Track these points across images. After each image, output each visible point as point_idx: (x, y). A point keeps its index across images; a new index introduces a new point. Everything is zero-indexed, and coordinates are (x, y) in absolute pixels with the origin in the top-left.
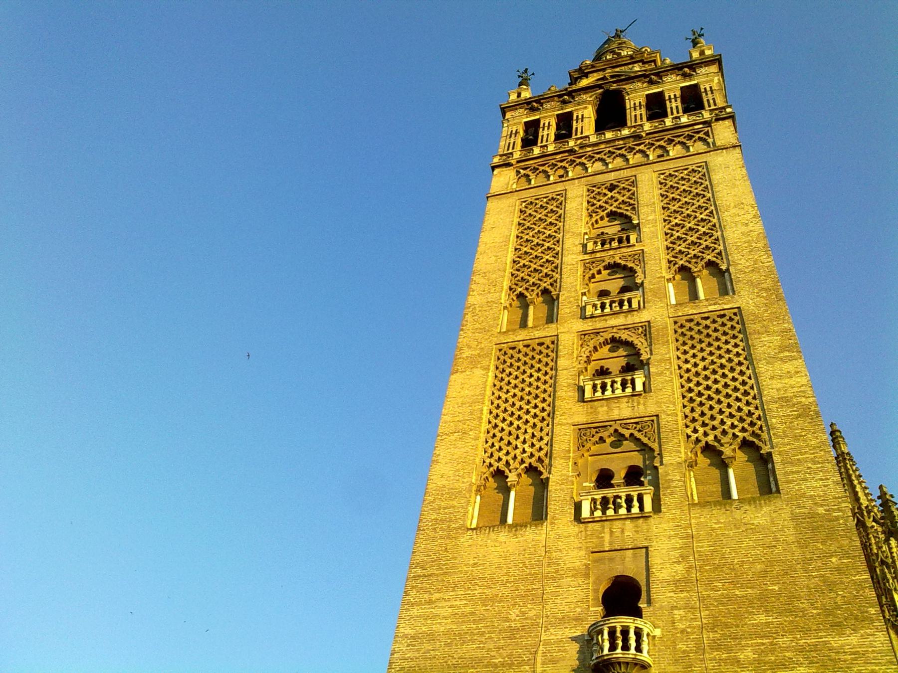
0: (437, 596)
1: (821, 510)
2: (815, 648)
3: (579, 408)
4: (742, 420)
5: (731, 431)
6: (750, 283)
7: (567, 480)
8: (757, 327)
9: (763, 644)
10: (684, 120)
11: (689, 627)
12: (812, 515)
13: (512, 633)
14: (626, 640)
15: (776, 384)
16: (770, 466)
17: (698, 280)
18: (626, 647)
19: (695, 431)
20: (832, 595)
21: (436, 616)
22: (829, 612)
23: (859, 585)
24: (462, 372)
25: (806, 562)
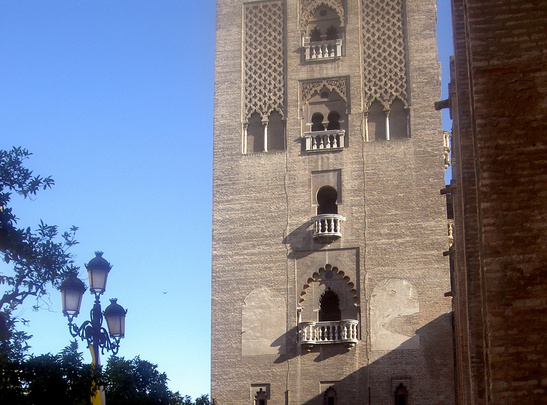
0: (231, 197)
1: (429, 149)
4: (396, 83)
5: (390, 91)
7: (298, 123)
9: (392, 225)
11: (359, 216)
13: (273, 219)
14: (329, 226)
16: (408, 117)
18: (329, 230)
20: (427, 200)
21: (233, 209)
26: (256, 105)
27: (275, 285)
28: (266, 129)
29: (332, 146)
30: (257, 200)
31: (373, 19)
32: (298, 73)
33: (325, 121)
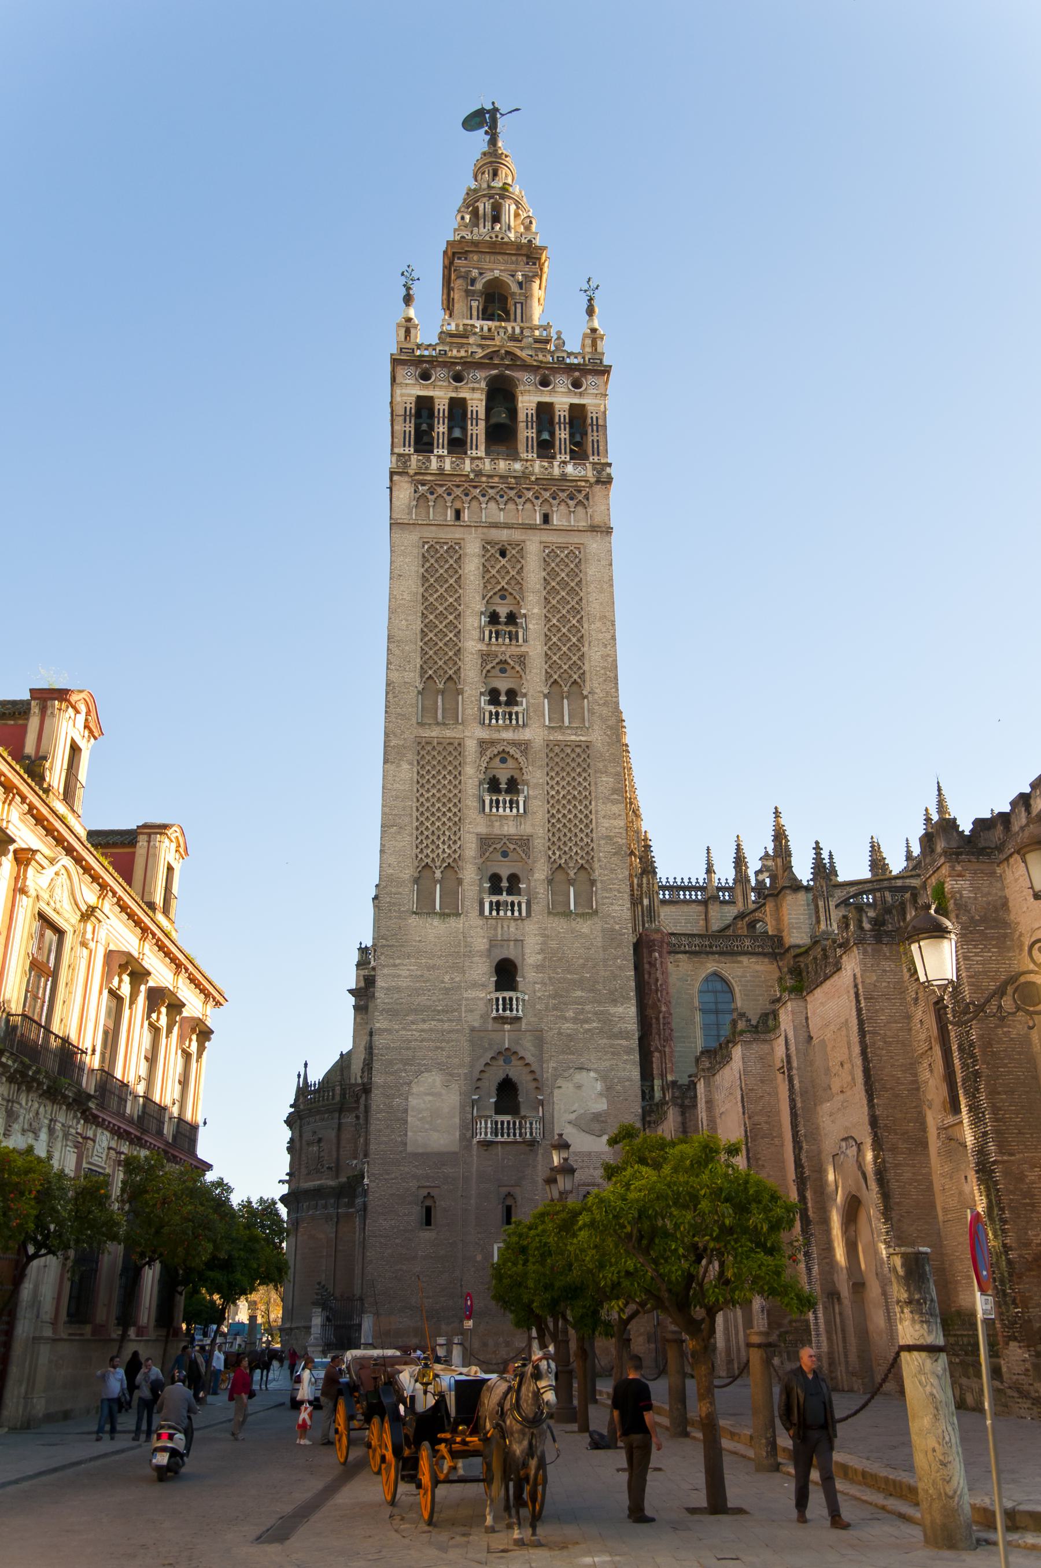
0: (398, 961)
1: (617, 927)
2: (602, 1013)
3: (480, 819)
4: (582, 848)
6: (601, 716)
8: (600, 765)
10: (570, 469)
12: (613, 930)
13: (447, 991)
14: (511, 1005)
15: (606, 823)
17: (565, 701)
18: (511, 1010)
19: (554, 853)
21: (399, 976)
22: (611, 993)
23: (628, 978)
24: (393, 763)
25: (605, 960)
26: (427, 856)
27: (448, 1068)
28: (438, 886)
29: (513, 914)
30: (431, 968)
31: (557, 773)
32: (475, 826)
33: (505, 884)
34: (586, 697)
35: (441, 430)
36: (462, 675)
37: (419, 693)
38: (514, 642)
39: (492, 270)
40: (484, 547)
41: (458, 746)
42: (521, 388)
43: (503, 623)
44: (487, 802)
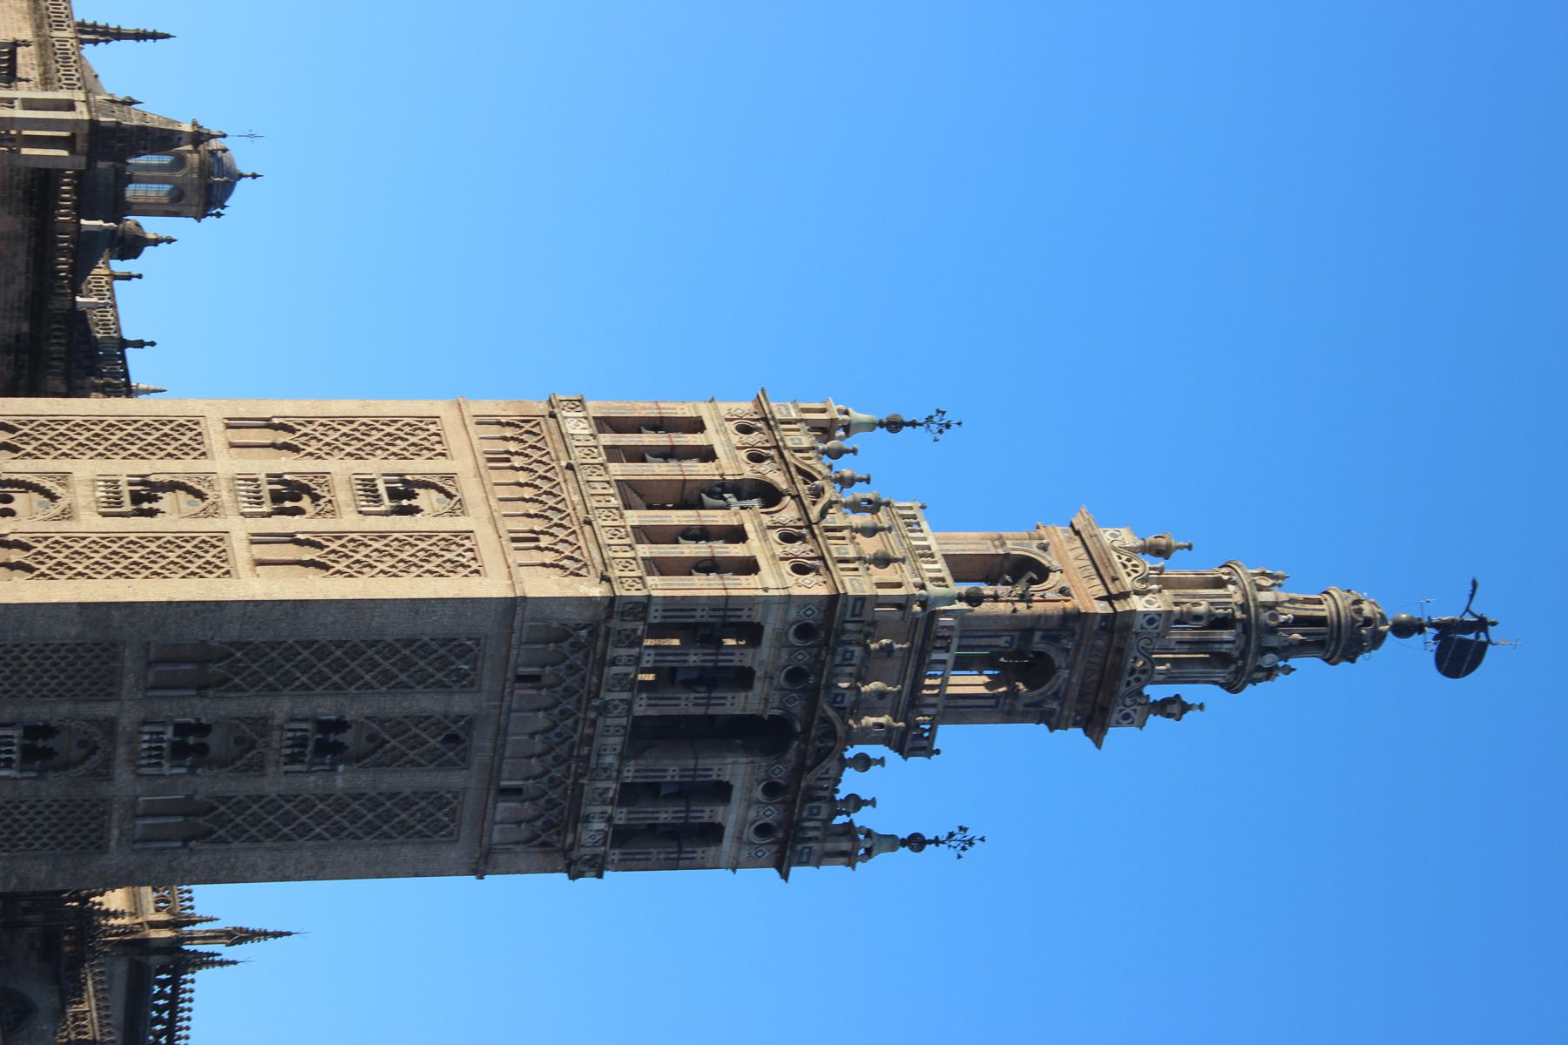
17: (180, 819)
34: (185, 841)
35: (692, 658)
36: (232, 695)
37: (204, 642)
38: (283, 760)
39: (1070, 667)
40: (462, 717)
41: (108, 693)
42: (763, 762)
43: (327, 744)
44: (9, 732)
